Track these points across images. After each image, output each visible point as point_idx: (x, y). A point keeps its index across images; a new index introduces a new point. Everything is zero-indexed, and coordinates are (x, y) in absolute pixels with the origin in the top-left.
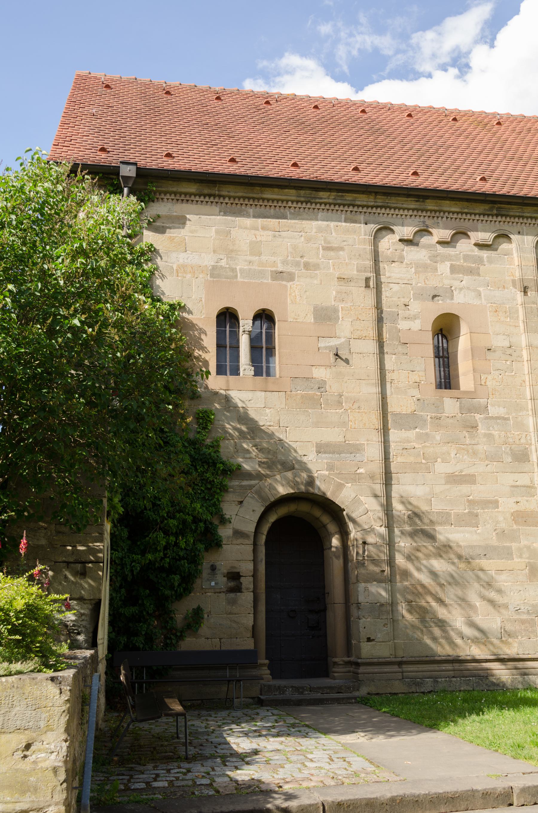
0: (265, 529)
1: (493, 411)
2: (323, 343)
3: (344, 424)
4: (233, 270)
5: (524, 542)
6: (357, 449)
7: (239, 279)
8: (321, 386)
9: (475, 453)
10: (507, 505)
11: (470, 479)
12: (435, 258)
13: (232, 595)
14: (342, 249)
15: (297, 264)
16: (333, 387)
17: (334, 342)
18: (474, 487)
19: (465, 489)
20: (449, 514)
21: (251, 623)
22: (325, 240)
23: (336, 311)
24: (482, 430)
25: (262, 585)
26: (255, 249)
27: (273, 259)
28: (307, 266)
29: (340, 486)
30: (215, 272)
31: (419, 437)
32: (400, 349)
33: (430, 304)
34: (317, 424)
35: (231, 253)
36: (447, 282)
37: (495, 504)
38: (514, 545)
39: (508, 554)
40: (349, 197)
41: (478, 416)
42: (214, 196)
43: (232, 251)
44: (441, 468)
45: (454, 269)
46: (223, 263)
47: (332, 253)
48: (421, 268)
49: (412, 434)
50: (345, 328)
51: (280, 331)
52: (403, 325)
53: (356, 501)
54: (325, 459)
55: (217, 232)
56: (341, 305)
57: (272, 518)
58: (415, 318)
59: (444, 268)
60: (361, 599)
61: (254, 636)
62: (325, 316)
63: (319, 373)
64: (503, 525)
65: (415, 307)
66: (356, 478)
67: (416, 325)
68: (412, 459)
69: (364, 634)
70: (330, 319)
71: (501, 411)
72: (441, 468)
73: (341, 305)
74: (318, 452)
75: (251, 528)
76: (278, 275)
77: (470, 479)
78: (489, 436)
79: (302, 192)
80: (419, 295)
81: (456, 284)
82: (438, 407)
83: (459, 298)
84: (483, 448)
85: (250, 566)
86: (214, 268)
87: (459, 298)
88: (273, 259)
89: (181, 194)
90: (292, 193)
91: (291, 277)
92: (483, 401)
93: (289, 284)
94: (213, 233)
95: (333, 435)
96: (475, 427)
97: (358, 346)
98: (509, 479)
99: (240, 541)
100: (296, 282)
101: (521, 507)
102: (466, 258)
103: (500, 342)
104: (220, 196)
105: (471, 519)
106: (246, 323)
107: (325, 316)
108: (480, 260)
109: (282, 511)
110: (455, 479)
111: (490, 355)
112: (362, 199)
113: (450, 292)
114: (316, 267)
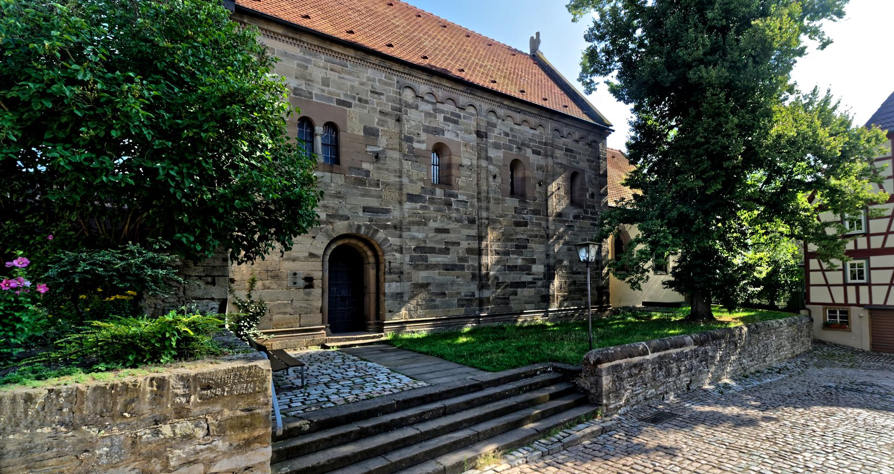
0: (329, 252)
1: (460, 198)
2: (369, 149)
3: (381, 197)
4: (311, 93)
5: (470, 263)
6: (387, 211)
7: (314, 100)
8: (367, 173)
9: (450, 218)
10: (464, 245)
11: (447, 231)
12: (435, 110)
13: (308, 290)
14: (382, 94)
15: (354, 98)
16: (374, 175)
17: (376, 149)
18: (449, 235)
19: (444, 236)
20: (435, 248)
21: (320, 305)
22: (372, 87)
23: (378, 131)
24: (454, 206)
25: (327, 284)
26: (326, 82)
27: (338, 91)
28: (360, 100)
29: (377, 231)
30: (296, 91)
31: (422, 208)
32: (414, 159)
33: (431, 136)
34: (363, 195)
35: (309, 81)
36: (441, 126)
37: (459, 244)
38: (466, 264)
39: (462, 268)
40: (388, 64)
41: (452, 199)
42: (296, 40)
43: (310, 80)
44: (432, 224)
45: (446, 119)
46: (303, 87)
47: (376, 96)
48: (428, 114)
49: (419, 205)
50: (383, 141)
51: (343, 138)
52: (416, 145)
53: (386, 240)
54: (368, 215)
55: (298, 65)
56: (380, 128)
57: (334, 247)
58: (423, 142)
59: (440, 117)
60: (387, 291)
61: (321, 312)
62: (371, 133)
63: (366, 166)
64: (461, 255)
65: (424, 136)
66: (385, 227)
67: (423, 147)
68: (417, 219)
69: (387, 308)
70: (374, 135)
71: (464, 198)
72: (432, 224)
73: (380, 128)
74: (364, 211)
75: (321, 252)
76: (340, 102)
77: (447, 231)
78: (457, 210)
79: (359, 53)
80: (427, 130)
81: (446, 127)
82: (433, 192)
83: (448, 135)
84: (454, 215)
85: (320, 274)
86: (295, 89)
87: (448, 135)
88: (338, 91)
89: (270, 32)
90: (351, 53)
91: (349, 105)
92: (456, 191)
93: (348, 109)
94: (295, 66)
95: (373, 203)
96: (451, 205)
97: (390, 153)
98: (466, 232)
99: (313, 259)
100: (352, 109)
101: (471, 246)
102: (452, 114)
103: (466, 162)
104: (300, 41)
105: (446, 251)
106: (319, 129)
107: (371, 133)
108: (459, 117)
109: (340, 243)
110: (439, 231)
111: (461, 168)
112: (396, 67)
113: (442, 132)
114: (366, 102)
